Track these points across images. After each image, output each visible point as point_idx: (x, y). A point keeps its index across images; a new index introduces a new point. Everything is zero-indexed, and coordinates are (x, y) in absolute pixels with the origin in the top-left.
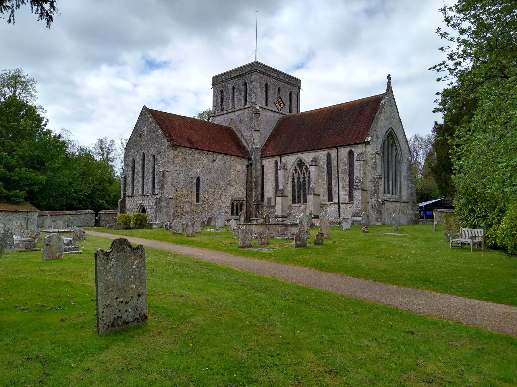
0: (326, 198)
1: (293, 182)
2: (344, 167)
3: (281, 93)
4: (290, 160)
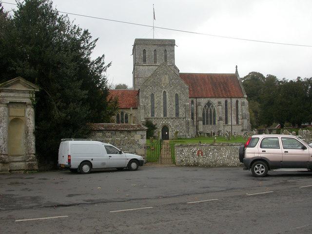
2: (234, 108)
4: (203, 101)
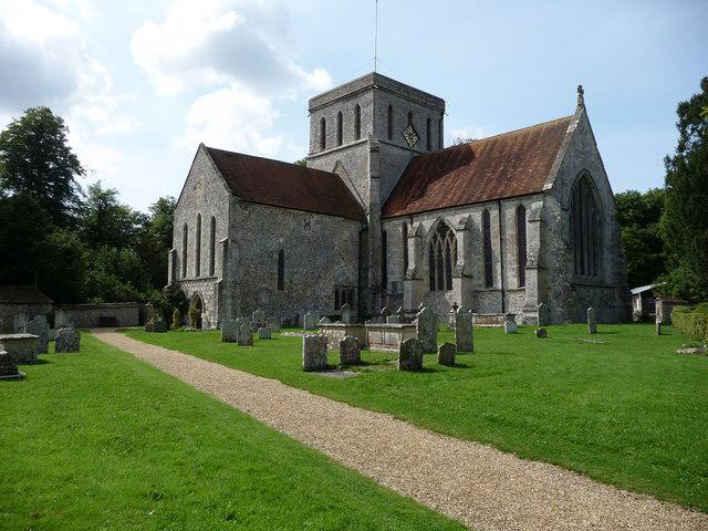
0: (482, 281)
1: (431, 257)
2: (511, 232)
3: (414, 121)
